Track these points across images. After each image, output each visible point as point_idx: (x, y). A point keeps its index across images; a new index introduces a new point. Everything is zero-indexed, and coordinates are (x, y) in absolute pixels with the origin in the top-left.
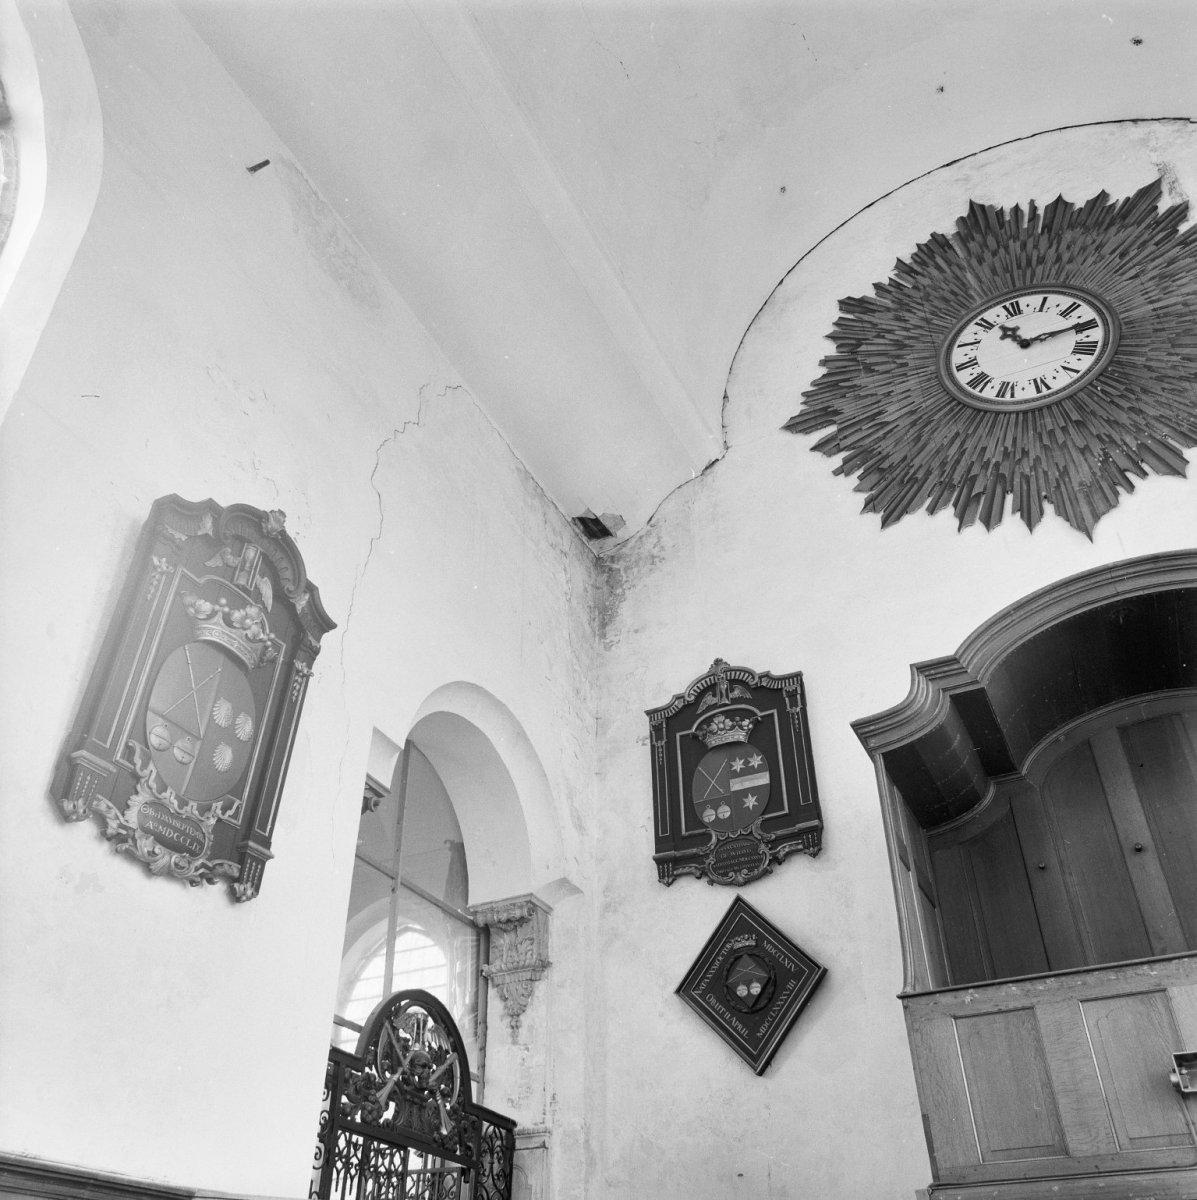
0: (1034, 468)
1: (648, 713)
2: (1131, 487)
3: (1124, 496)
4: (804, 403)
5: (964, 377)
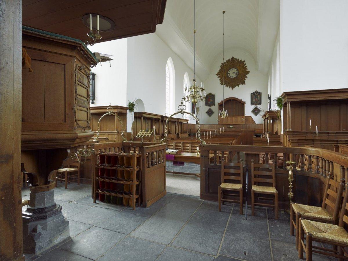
5: (228, 74)
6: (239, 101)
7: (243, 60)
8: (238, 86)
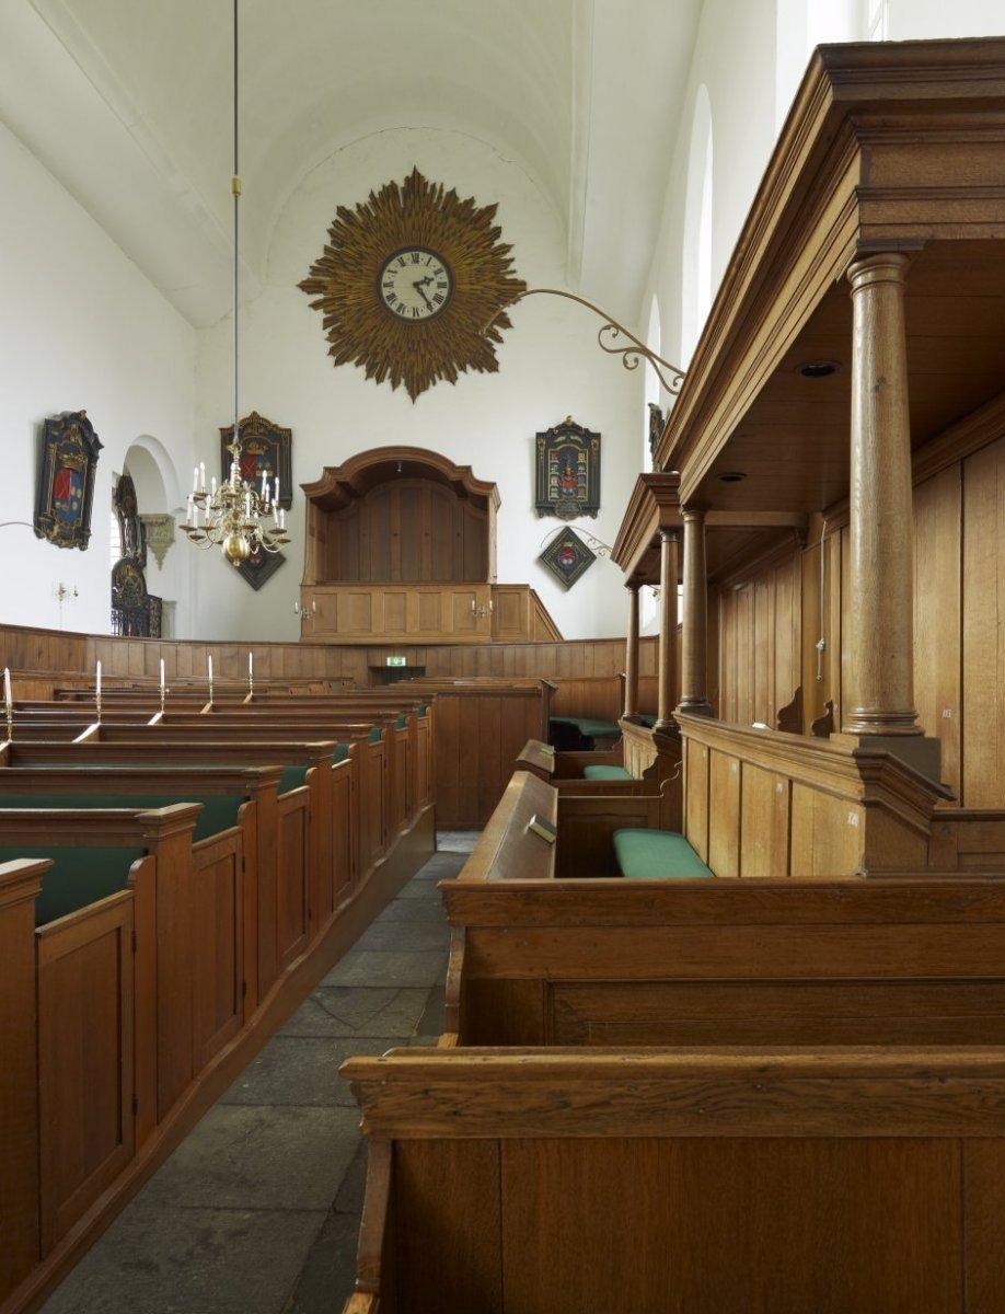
0: (402, 357)
1: (221, 429)
2: (434, 383)
3: (431, 386)
4: (311, 274)
5: (386, 292)
6: (453, 476)
7: (480, 204)
8: (452, 379)
